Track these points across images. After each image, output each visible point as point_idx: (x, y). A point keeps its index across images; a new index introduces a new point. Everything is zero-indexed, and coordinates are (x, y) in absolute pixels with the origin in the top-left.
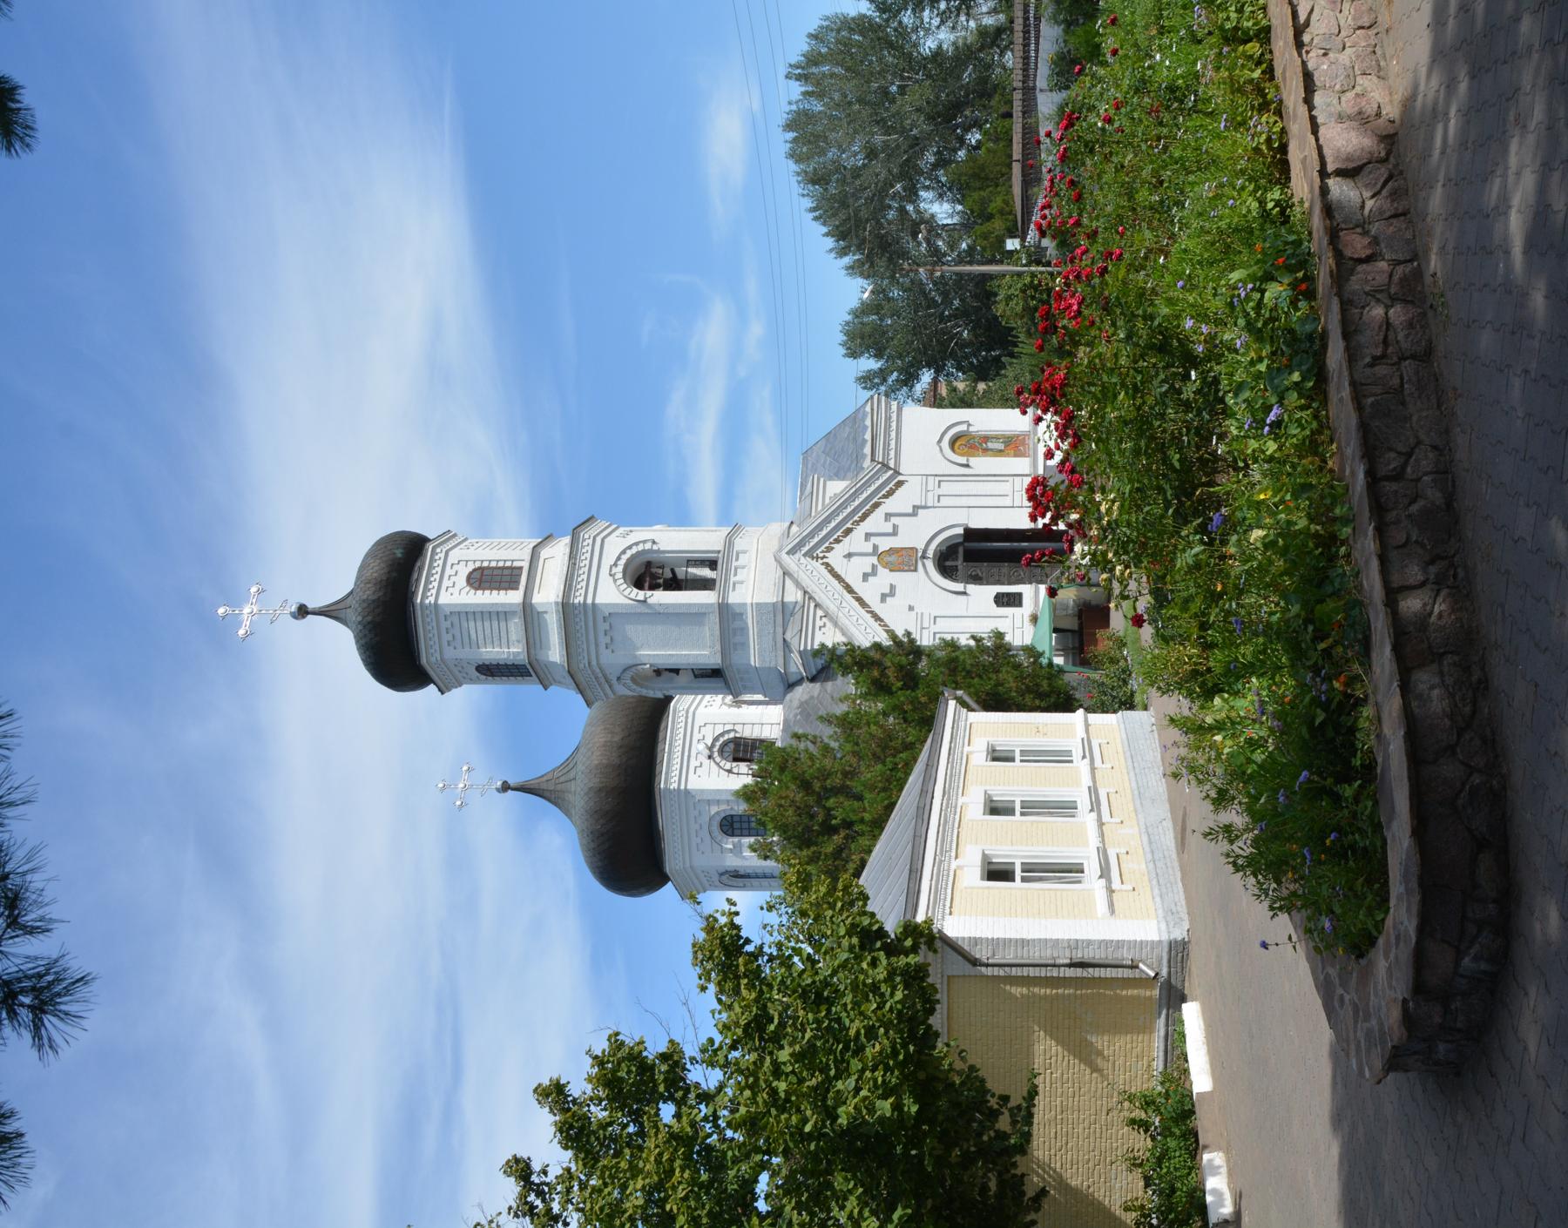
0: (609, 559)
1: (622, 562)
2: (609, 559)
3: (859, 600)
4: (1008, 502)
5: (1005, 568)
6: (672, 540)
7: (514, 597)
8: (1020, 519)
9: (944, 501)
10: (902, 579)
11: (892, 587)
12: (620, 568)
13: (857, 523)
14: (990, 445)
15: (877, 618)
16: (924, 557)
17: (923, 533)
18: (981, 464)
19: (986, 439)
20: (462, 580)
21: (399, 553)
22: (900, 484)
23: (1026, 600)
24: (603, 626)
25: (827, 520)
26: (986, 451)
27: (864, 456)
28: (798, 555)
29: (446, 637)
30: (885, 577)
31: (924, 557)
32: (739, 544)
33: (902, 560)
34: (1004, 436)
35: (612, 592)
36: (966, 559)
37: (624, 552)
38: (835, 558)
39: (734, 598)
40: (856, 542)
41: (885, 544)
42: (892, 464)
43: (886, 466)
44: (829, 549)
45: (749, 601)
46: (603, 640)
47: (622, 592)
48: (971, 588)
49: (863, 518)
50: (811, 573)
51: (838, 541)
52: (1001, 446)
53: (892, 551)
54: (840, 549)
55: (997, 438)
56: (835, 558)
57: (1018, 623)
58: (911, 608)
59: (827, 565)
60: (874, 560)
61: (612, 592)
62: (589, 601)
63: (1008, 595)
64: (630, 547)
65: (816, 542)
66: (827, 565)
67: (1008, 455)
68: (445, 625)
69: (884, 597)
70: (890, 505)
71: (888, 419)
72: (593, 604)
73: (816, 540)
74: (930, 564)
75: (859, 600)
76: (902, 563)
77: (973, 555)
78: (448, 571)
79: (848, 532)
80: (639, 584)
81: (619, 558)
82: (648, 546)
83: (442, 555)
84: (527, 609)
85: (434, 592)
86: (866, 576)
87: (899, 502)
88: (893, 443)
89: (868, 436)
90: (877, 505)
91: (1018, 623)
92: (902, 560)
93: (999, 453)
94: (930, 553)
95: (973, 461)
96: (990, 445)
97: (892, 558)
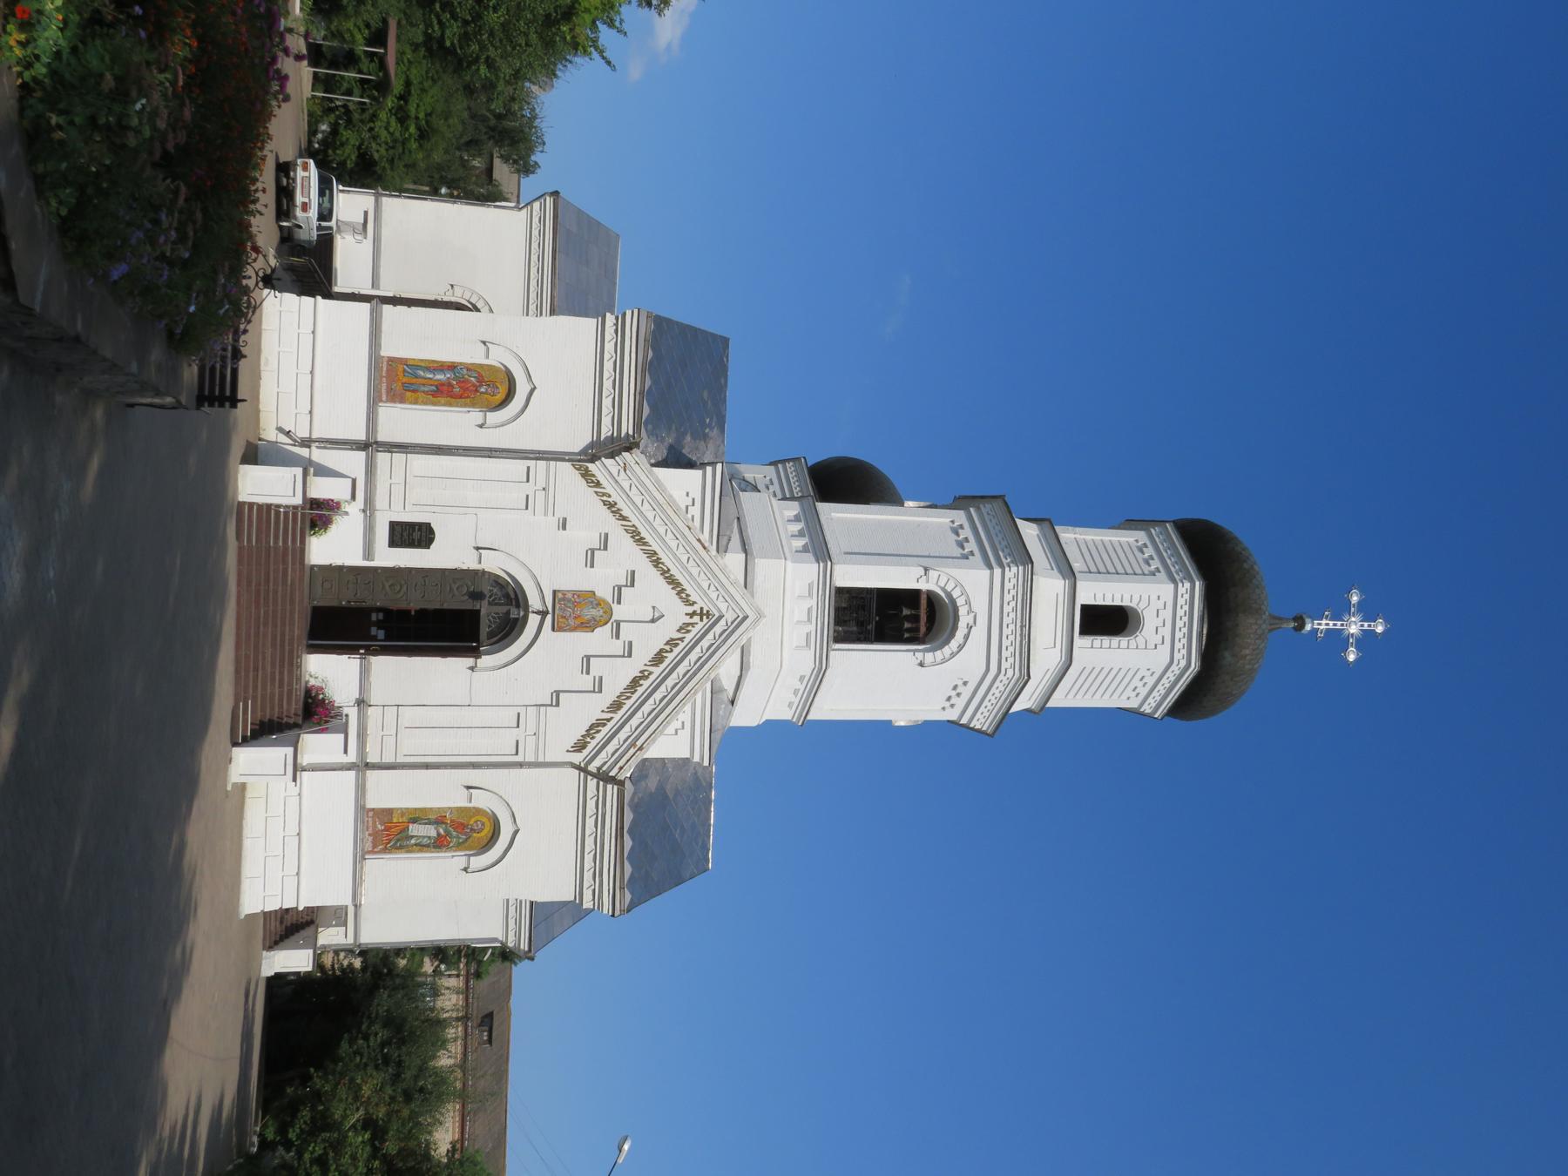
0: (979, 634)
1: (960, 635)
2: (979, 634)
3: (640, 541)
5: (414, 603)
6: (888, 686)
8: (386, 667)
9: (509, 716)
10: (575, 579)
12: (962, 624)
13: (644, 676)
14: (431, 831)
15: (611, 506)
16: (543, 614)
17: (542, 660)
19: (439, 844)
20: (1150, 622)
21: (1227, 657)
22: (580, 746)
23: (382, 534)
24: (972, 546)
25: (690, 676)
26: (439, 821)
27: (635, 808)
28: (730, 616)
29: (1149, 551)
30: (600, 581)
31: (543, 614)
32: (805, 662)
33: (578, 611)
34: (408, 849)
35: (970, 585)
36: (475, 614)
37: (961, 647)
38: (676, 613)
39: (809, 570)
40: (648, 641)
41: (599, 640)
42: (592, 783)
43: (603, 777)
44: (684, 628)
45: (789, 563)
46: (967, 532)
47: (958, 584)
48: (468, 562)
49: (635, 683)
51: (672, 643)
52: (414, 829)
53: (589, 626)
54: (668, 629)
55: (422, 847)
56: (676, 613)
58: (564, 525)
59: (688, 602)
60: (619, 612)
61: (970, 585)
62: (997, 571)
63: (411, 544)
64: (953, 655)
65: (709, 629)
66: (688, 602)
67: (403, 812)
68: (1156, 564)
70: (595, 707)
71: (598, 874)
72: (990, 567)
73: (705, 643)
74: (534, 602)
75: (640, 541)
78: (1167, 631)
79: (658, 659)
80: (932, 598)
81: (967, 637)
82: (929, 657)
83: (1177, 656)
84: (1068, 572)
85: (1181, 601)
87: (582, 711)
88: (590, 822)
89: (628, 843)
90: (616, 706)
92: (578, 611)
93: (417, 817)
94: (534, 620)
95: (458, 800)
96: (431, 831)
97: (591, 613)
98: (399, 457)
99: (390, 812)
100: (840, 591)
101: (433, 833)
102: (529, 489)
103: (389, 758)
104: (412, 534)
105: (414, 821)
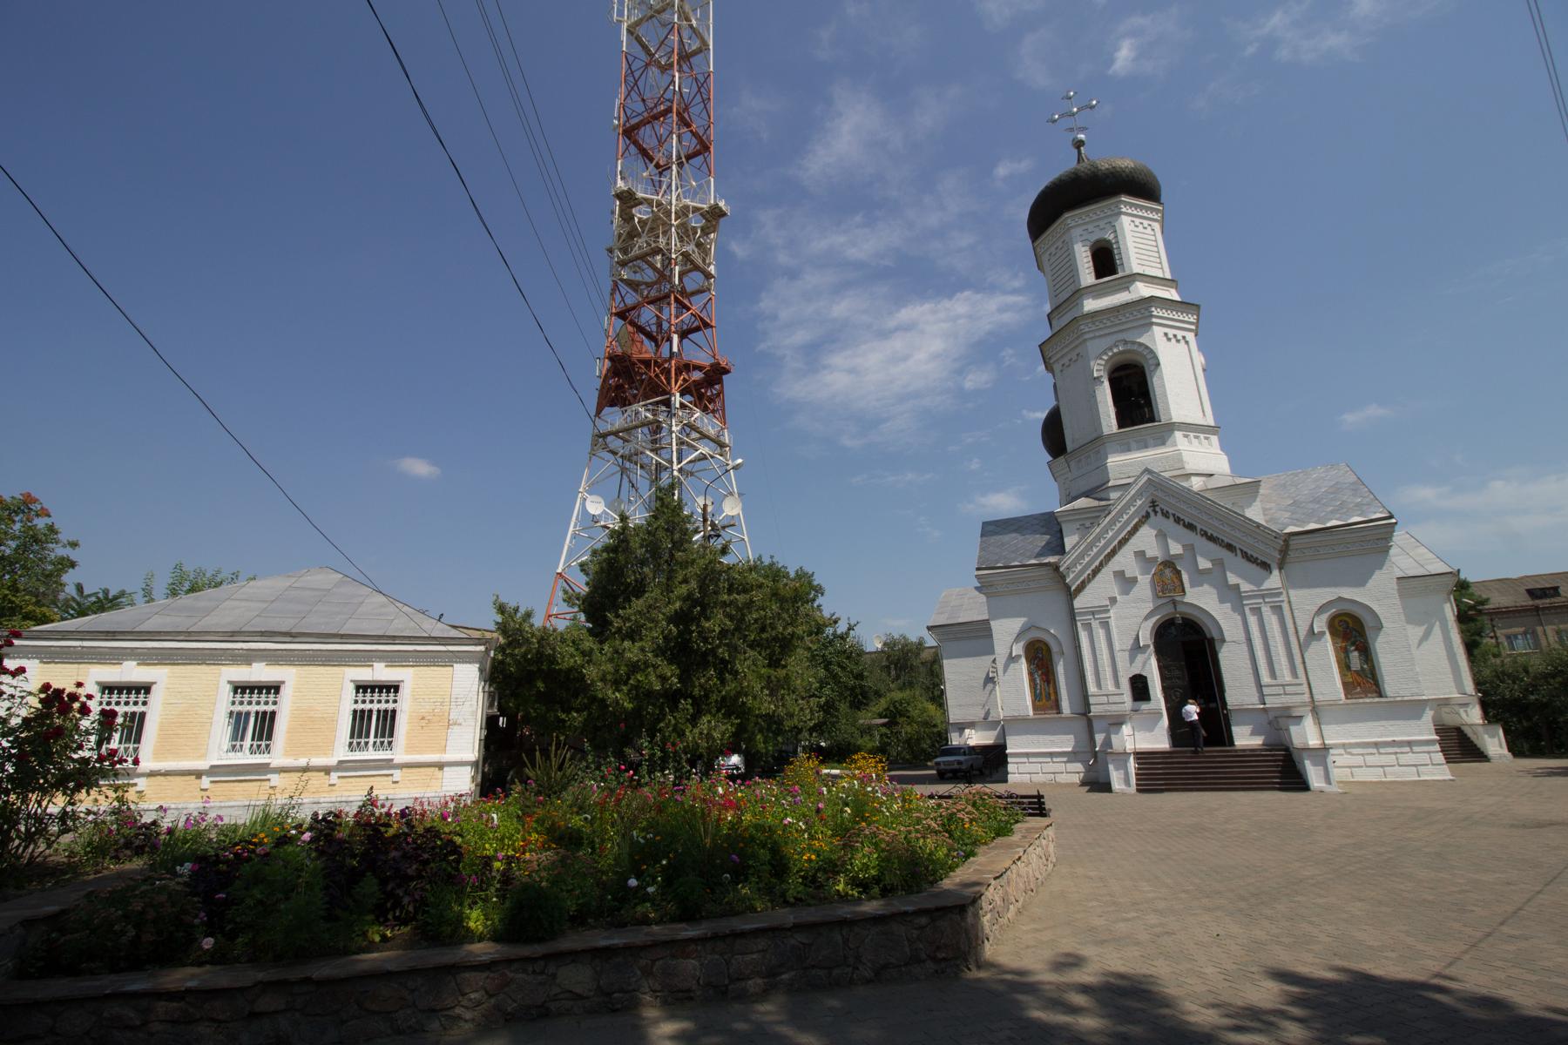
3: (1113, 553)
4: (1266, 679)
7: (1087, 276)
11: (1134, 581)
13: (1205, 534)
15: (1096, 572)
17: (1202, 598)
18: (1325, 652)
22: (1266, 566)
26: (1346, 651)
44: (1166, 515)
46: (1065, 361)
49: (1211, 538)
50: (1126, 506)
57: (1112, 699)
67: (1343, 675)
69: (1120, 575)
74: (1169, 609)
76: (1164, 584)
77: (1188, 652)
79: (1190, 527)
86: (1140, 555)
90: (1230, 547)
91: (1112, 699)
93: (1345, 666)
94: (1180, 608)
98: (1092, 700)
99: (1345, 684)
100: (1121, 425)
101: (1356, 654)
102: (1095, 624)
103: (1305, 688)
104: (1139, 688)
105: (1348, 667)
